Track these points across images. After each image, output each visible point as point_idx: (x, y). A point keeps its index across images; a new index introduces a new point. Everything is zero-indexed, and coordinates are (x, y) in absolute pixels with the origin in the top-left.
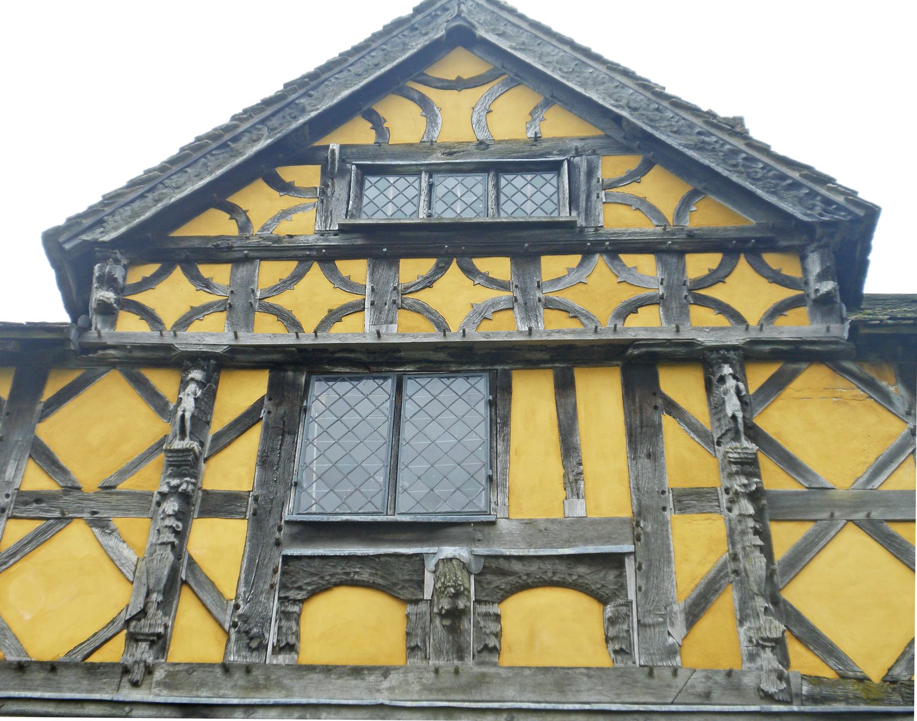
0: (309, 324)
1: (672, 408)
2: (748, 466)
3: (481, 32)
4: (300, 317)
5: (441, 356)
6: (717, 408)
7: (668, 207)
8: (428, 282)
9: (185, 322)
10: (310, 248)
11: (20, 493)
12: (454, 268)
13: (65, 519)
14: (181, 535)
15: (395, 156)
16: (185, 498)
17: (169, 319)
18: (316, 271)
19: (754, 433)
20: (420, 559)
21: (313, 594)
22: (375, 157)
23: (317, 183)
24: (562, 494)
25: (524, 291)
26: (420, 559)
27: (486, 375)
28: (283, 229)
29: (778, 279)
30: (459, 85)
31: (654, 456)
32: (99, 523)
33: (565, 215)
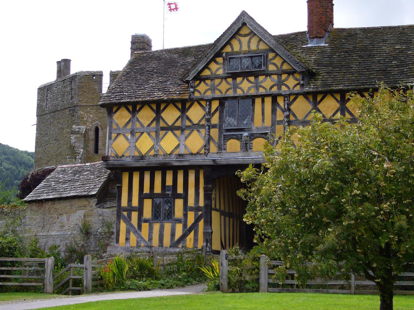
0: (224, 92)
1: (278, 104)
2: (288, 117)
3: (247, 25)
4: (222, 91)
5: (244, 97)
6: (285, 105)
7: (279, 65)
8: (241, 83)
9: (205, 93)
10: (222, 77)
11: (186, 126)
12: (245, 80)
13: (193, 130)
14: (209, 132)
15: (235, 55)
16: (209, 126)
17: (202, 92)
18: (224, 81)
19: (289, 110)
20: (242, 135)
21: (228, 140)
22: (232, 55)
23: (222, 62)
24: (262, 122)
25: (256, 84)
26: (242, 135)
27: (251, 99)
28: (218, 73)
29: (296, 79)
30: (246, 36)
31: (275, 114)
32: (198, 131)
33: (263, 68)
